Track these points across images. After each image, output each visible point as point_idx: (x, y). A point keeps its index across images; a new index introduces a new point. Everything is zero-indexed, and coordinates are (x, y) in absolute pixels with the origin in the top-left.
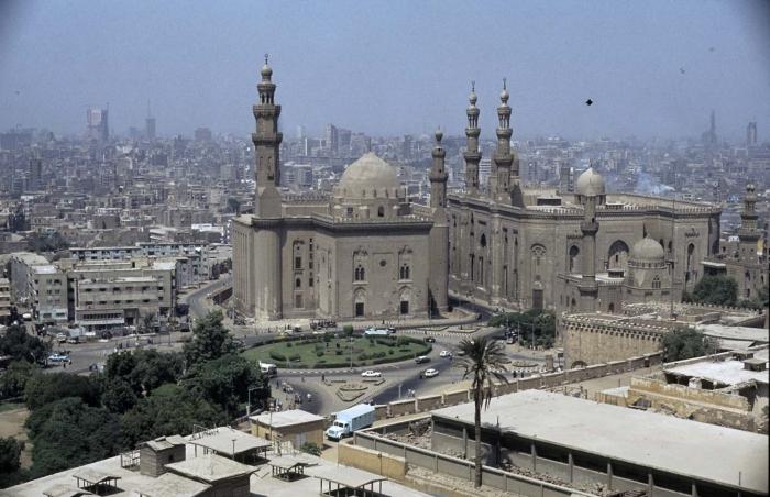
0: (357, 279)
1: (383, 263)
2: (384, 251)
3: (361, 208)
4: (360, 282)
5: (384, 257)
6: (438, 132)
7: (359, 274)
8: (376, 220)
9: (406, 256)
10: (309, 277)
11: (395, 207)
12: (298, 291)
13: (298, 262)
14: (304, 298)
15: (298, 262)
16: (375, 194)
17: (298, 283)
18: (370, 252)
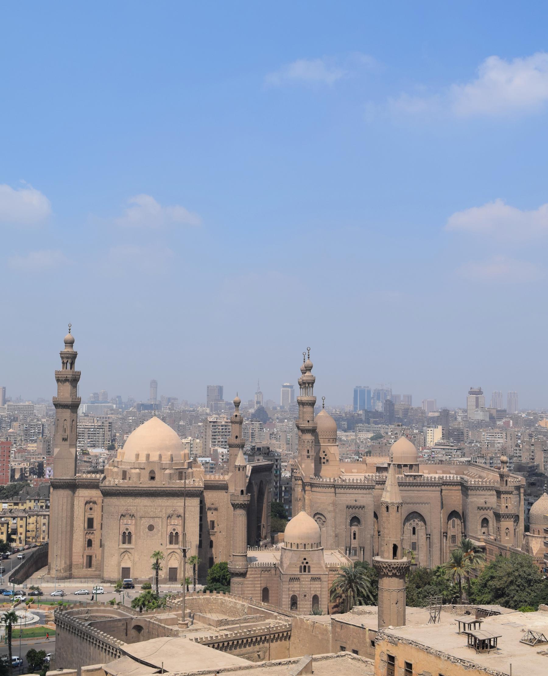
0: (124, 543)
1: (151, 528)
2: (152, 514)
3: (133, 471)
4: (126, 546)
5: (152, 523)
6: (237, 399)
7: (127, 537)
8: (146, 484)
9: (176, 521)
10: (99, 538)
11: (167, 471)
12: (88, 552)
13: (90, 522)
14: (94, 559)
15: (90, 522)
16: (148, 456)
17: (90, 543)
18: (138, 515)
